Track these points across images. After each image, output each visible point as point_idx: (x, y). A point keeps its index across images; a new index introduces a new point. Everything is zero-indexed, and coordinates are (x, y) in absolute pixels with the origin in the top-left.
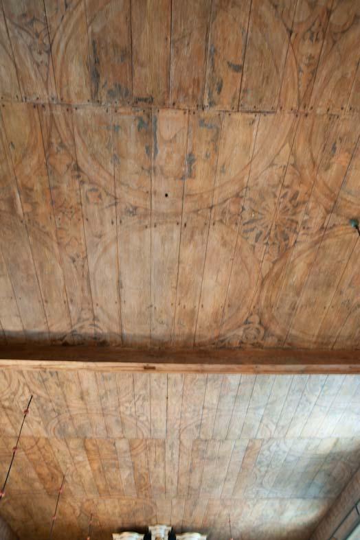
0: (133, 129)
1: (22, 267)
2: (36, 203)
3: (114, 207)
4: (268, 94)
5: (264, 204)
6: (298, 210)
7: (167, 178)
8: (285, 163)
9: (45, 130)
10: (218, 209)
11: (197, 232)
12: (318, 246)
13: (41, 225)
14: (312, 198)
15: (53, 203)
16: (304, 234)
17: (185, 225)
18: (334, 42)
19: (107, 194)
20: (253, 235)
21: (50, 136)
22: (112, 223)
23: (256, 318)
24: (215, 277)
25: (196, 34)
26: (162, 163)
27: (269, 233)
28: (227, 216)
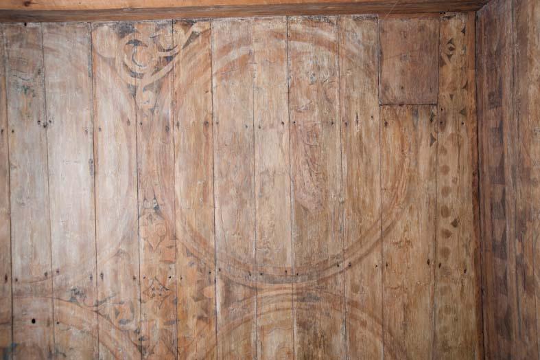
1: (232, 192)
2: (197, 300)
3: (100, 300)
13: (195, 266)
15: (175, 302)
19: (108, 318)
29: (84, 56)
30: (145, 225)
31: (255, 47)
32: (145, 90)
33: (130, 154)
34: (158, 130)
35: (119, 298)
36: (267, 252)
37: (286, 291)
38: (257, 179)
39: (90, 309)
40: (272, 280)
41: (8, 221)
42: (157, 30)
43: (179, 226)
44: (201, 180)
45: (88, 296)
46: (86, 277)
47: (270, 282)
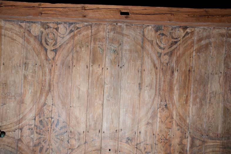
1: (198, 100)
2: (179, 145)
3: (138, 143)
5: (57, 145)
6: (37, 141)
11: (92, 127)
12: (21, 116)
13: (179, 132)
14: (31, 148)
15: (170, 145)
16: (32, 125)
17: (99, 132)
20: (61, 125)
22: (140, 132)
23: (51, 55)
24: (81, 93)
28: (76, 138)
29: (140, 38)
30: (160, 112)
31: (212, 40)
33: (156, 81)
34: (169, 72)
35: (146, 142)
36: (210, 126)
37: (217, 144)
38: (208, 95)
39: (134, 146)
40: (212, 139)
41: (102, 107)
42: (172, 30)
43: (174, 113)
44: (185, 94)
45: (133, 141)
46: (133, 133)
47: (210, 139)
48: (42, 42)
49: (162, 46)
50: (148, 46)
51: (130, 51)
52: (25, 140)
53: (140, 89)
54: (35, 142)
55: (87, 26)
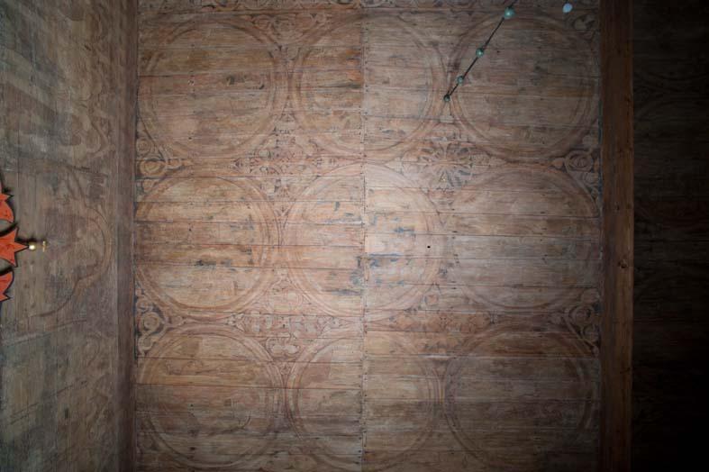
0: (378, 270)
1: (501, 367)
2: (438, 344)
4: (351, 184)
6: (438, 146)
7: (414, 247)
8: (400, 164)
9: (382, 328)
10: (440, 208)
11: (461, 222)
13: (457, 343)
14: (428, 138)
18: (322, 150)
21: (385, 326)
23: (557, 162)
25: (321, 231)
26: (403, 251)
27: (461, 165)
29: (583, 283)
32: (562, 318)
34: (538, 325)
38: (507, 380)
40: (447, 388)
42: (596, 327)
43: (482, 335)
48: (573, 151)
49: (574, 314)
50: (572, 294)
51: (567, 270)
52: (439, 130)
53: (515, 287)
54: (437, 142)
55: (598, 210)
